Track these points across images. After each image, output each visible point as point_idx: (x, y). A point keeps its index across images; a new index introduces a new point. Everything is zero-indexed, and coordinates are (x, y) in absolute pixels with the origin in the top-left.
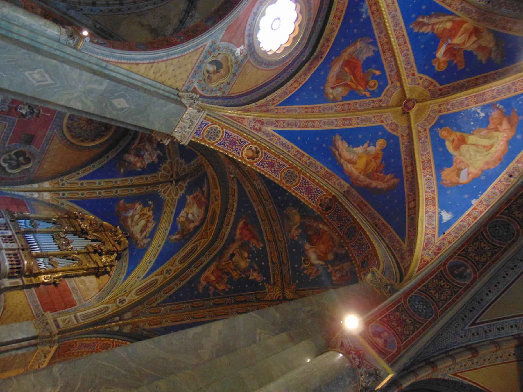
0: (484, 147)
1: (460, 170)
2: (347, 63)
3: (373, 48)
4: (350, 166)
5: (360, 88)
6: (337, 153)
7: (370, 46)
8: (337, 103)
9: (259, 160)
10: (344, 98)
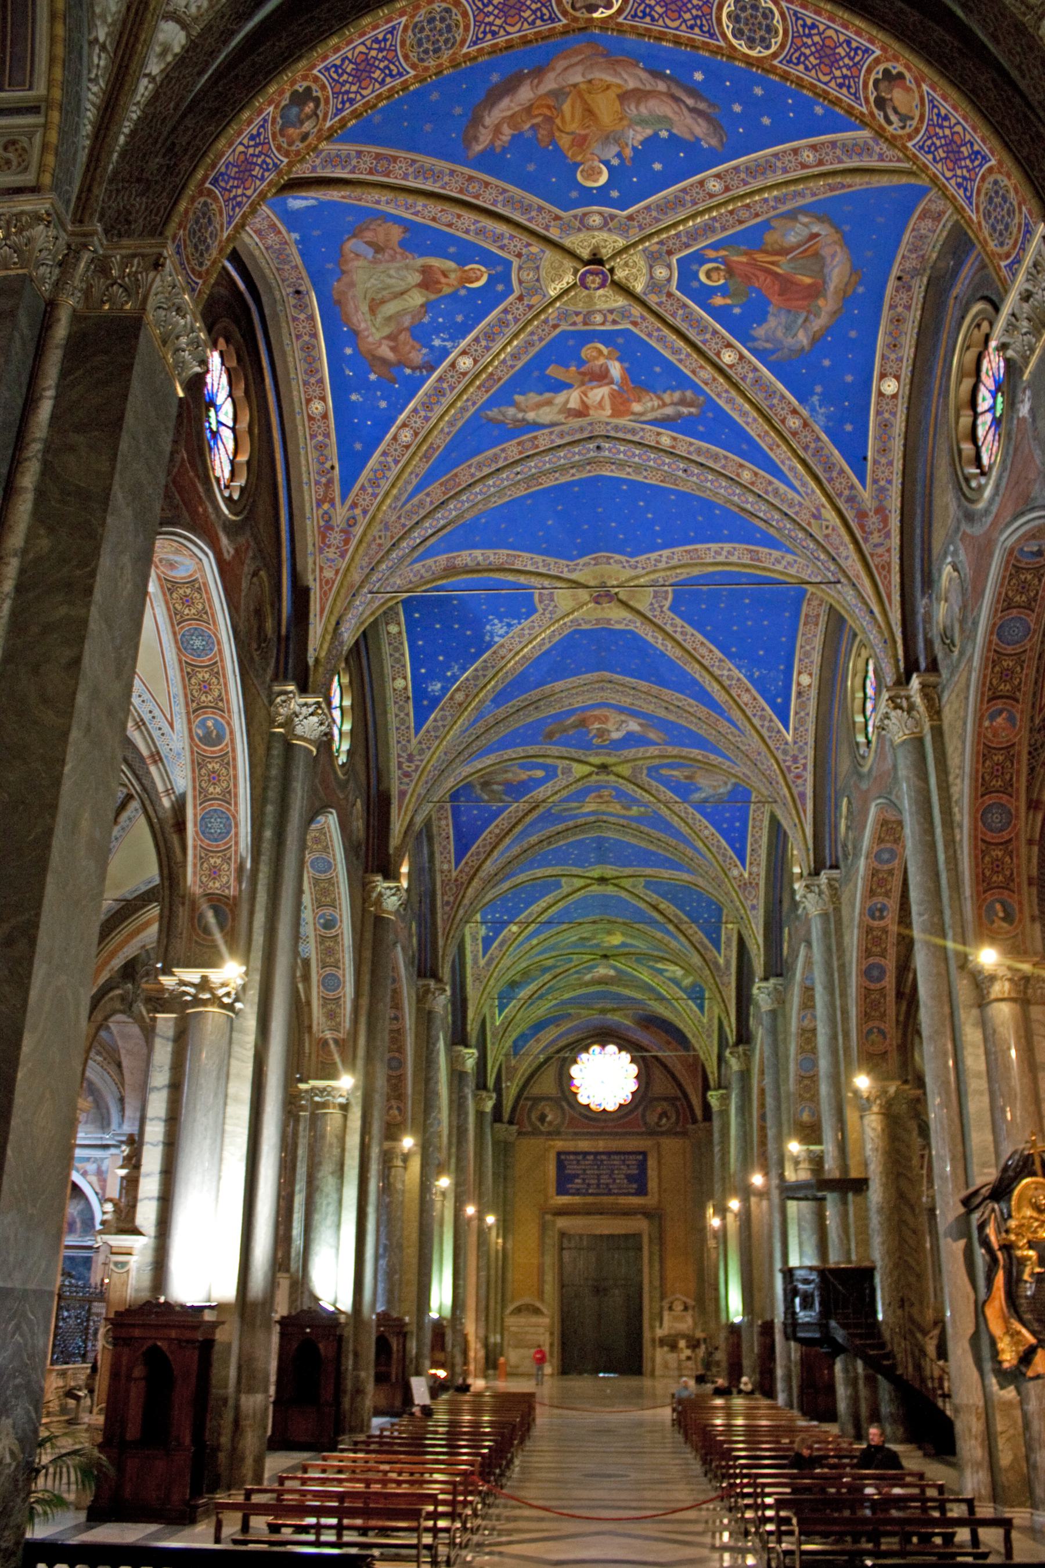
0: (383, 302)
1: (378, 249)
2: (815, 292)
3: (760, 345)
4: (632, 84)
5: (744, 259)
6: (690, 102)
7: (768, 346)
8: (772, 213)
9: (869, 71)
10: (766, 226)
